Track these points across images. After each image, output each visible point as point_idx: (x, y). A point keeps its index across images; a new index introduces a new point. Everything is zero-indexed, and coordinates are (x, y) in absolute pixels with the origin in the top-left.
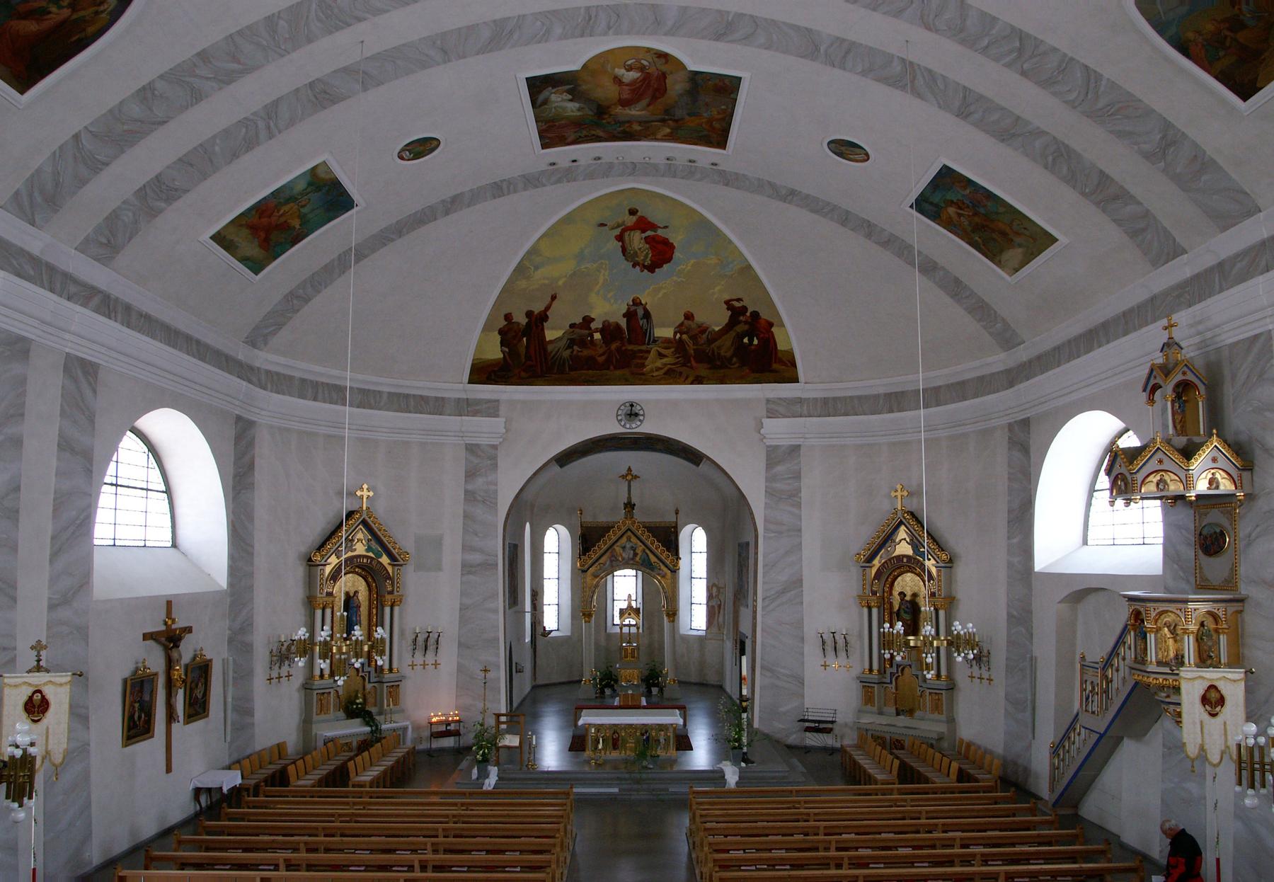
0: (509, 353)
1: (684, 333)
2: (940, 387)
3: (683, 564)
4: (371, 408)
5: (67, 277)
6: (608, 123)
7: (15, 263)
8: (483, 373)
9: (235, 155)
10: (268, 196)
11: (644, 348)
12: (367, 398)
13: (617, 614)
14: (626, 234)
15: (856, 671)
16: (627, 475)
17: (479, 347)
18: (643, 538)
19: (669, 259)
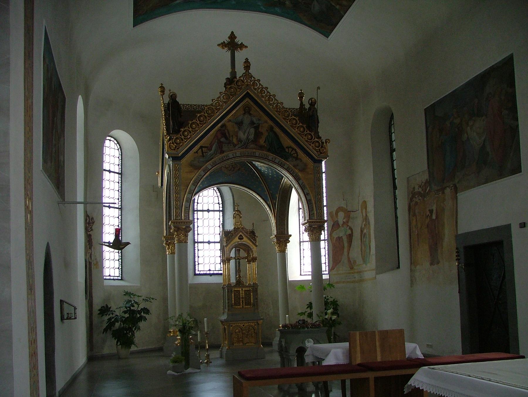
16: (229, 43)
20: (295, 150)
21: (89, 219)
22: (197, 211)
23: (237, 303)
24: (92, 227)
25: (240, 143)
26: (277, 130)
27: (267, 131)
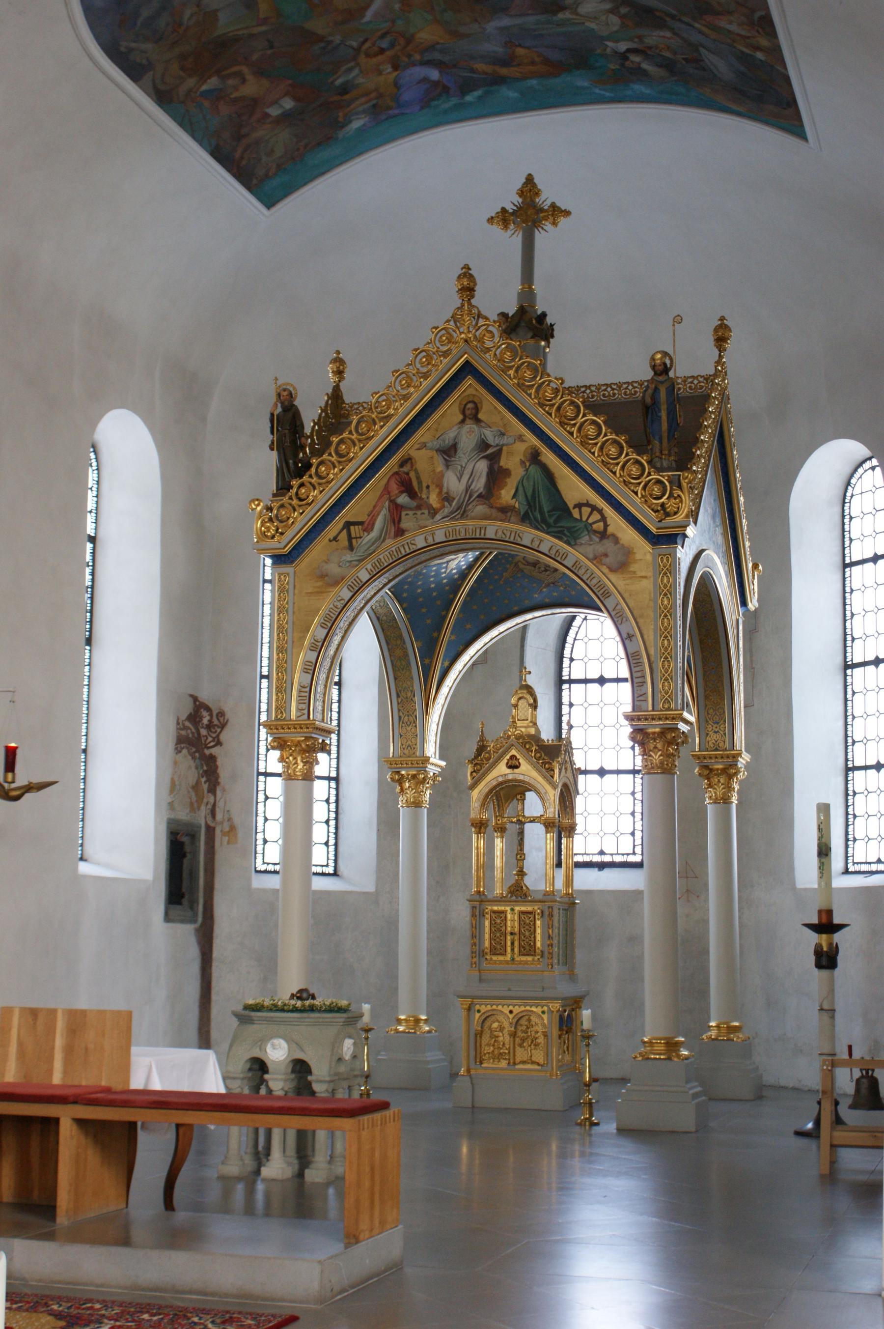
16: (520, 208)
20: (600, 511)
21: (211, 715)
22: (571, 681)
23: (498, 949)
24: (218, 736)
25: (446, 504)
26: (550, 458)
27: (522, 463)
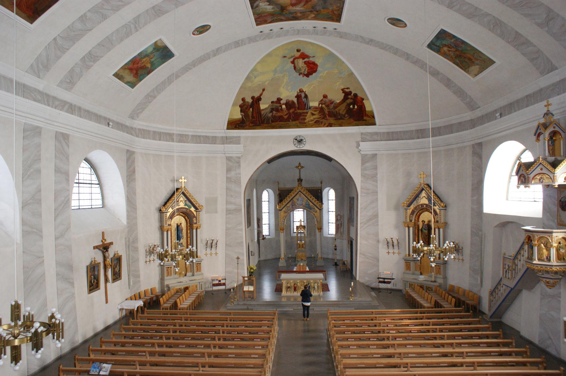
0: (244, 116)
1: (324, 104)
2: (441, 127)
3: (325, 206)
4: (184, 142)
5: (55, 98)
6: (286, 13)
7: (33, 94)
8: (233, 125)
9: (122, 40)
10: (137, 56)
11: (305, 111)
12: (183, 138)
13: (295, 228)
14: (296, 61)
15: (402, 255)
17: (231, 113)
18: (306, 195)
19: (315, 71)
23: (300, 247)
